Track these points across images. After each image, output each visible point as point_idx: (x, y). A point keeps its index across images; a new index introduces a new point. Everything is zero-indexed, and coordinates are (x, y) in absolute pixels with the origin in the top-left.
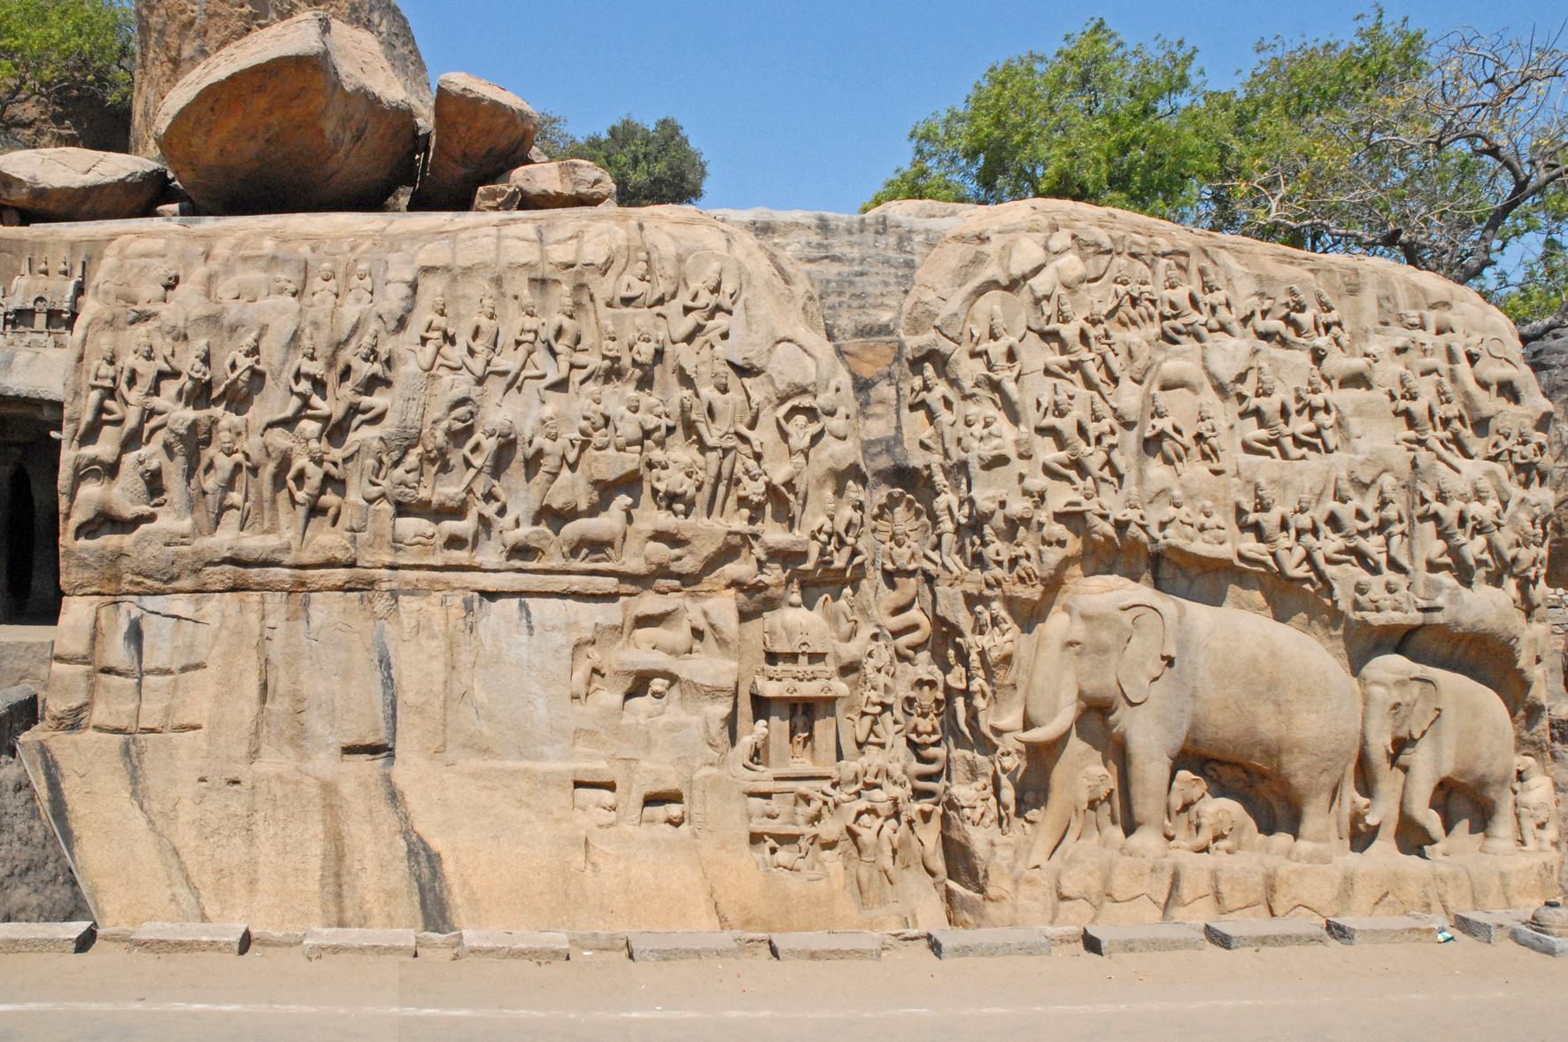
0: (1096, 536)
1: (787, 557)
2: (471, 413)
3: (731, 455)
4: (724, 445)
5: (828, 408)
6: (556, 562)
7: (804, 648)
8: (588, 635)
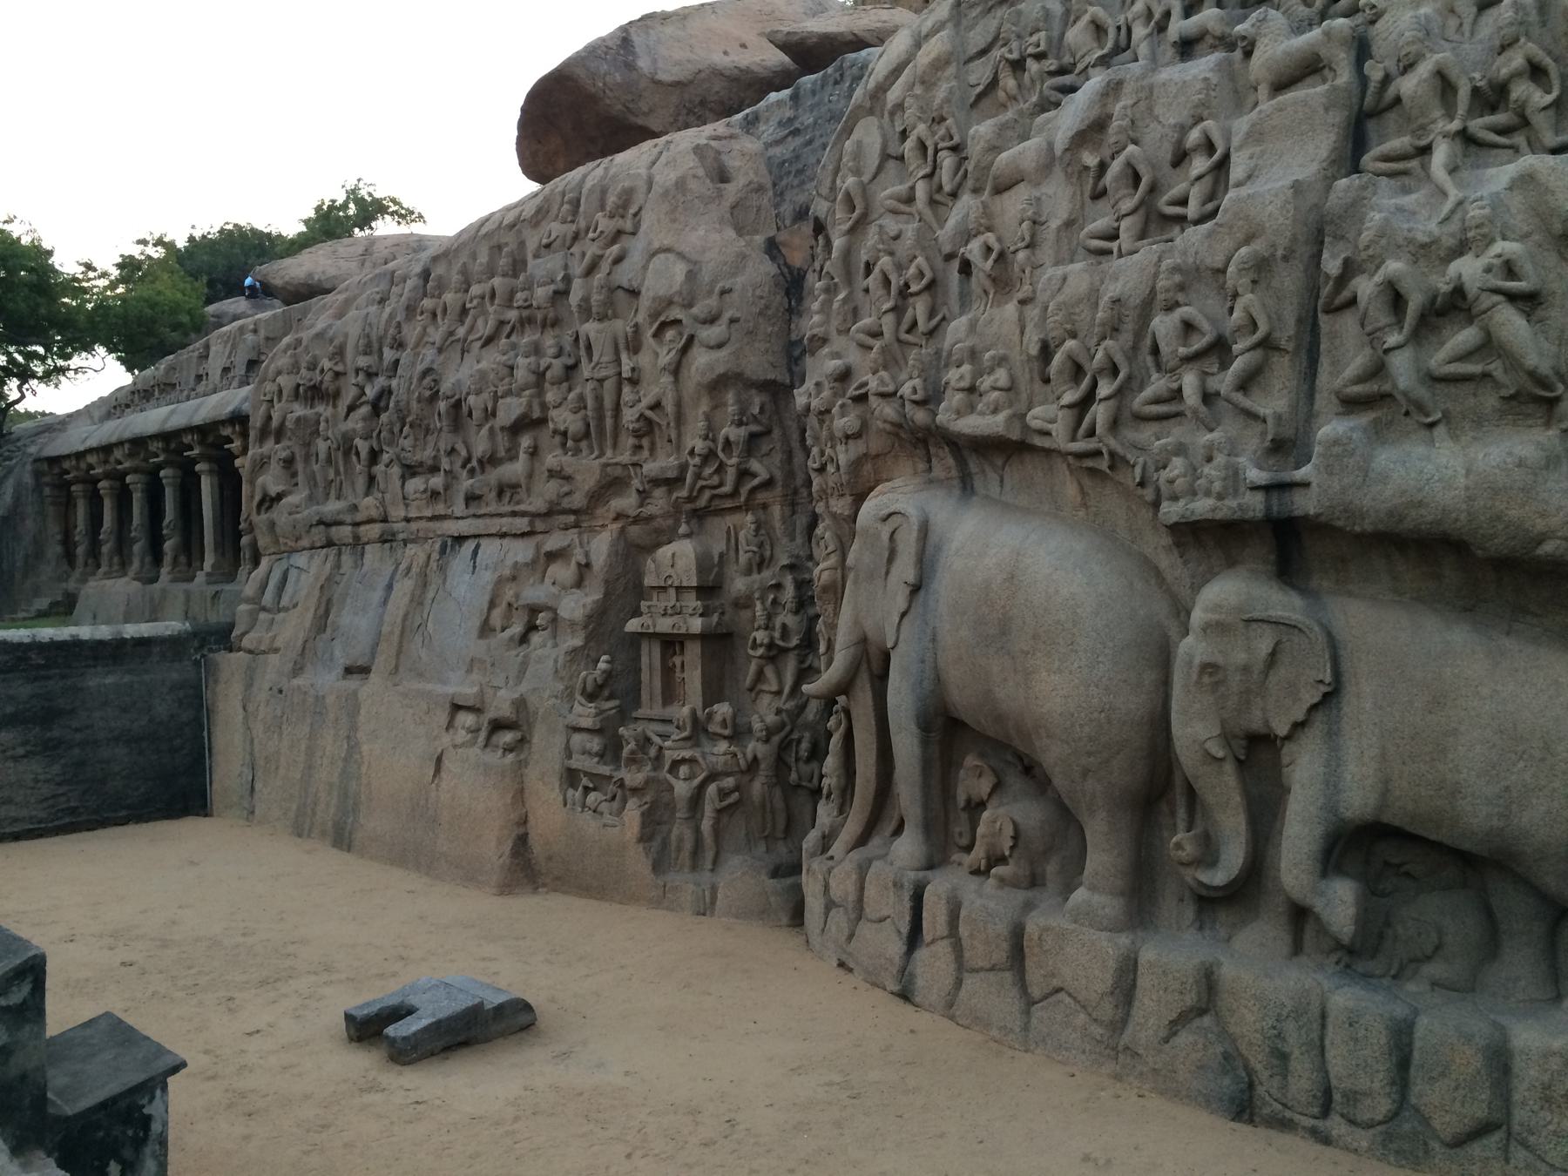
0: (880, 424)
1: (672, 483)
3: (608, 385)
4: (597, 376)
5: (702, 316)
6: (492, 509)
8: (507, 572)
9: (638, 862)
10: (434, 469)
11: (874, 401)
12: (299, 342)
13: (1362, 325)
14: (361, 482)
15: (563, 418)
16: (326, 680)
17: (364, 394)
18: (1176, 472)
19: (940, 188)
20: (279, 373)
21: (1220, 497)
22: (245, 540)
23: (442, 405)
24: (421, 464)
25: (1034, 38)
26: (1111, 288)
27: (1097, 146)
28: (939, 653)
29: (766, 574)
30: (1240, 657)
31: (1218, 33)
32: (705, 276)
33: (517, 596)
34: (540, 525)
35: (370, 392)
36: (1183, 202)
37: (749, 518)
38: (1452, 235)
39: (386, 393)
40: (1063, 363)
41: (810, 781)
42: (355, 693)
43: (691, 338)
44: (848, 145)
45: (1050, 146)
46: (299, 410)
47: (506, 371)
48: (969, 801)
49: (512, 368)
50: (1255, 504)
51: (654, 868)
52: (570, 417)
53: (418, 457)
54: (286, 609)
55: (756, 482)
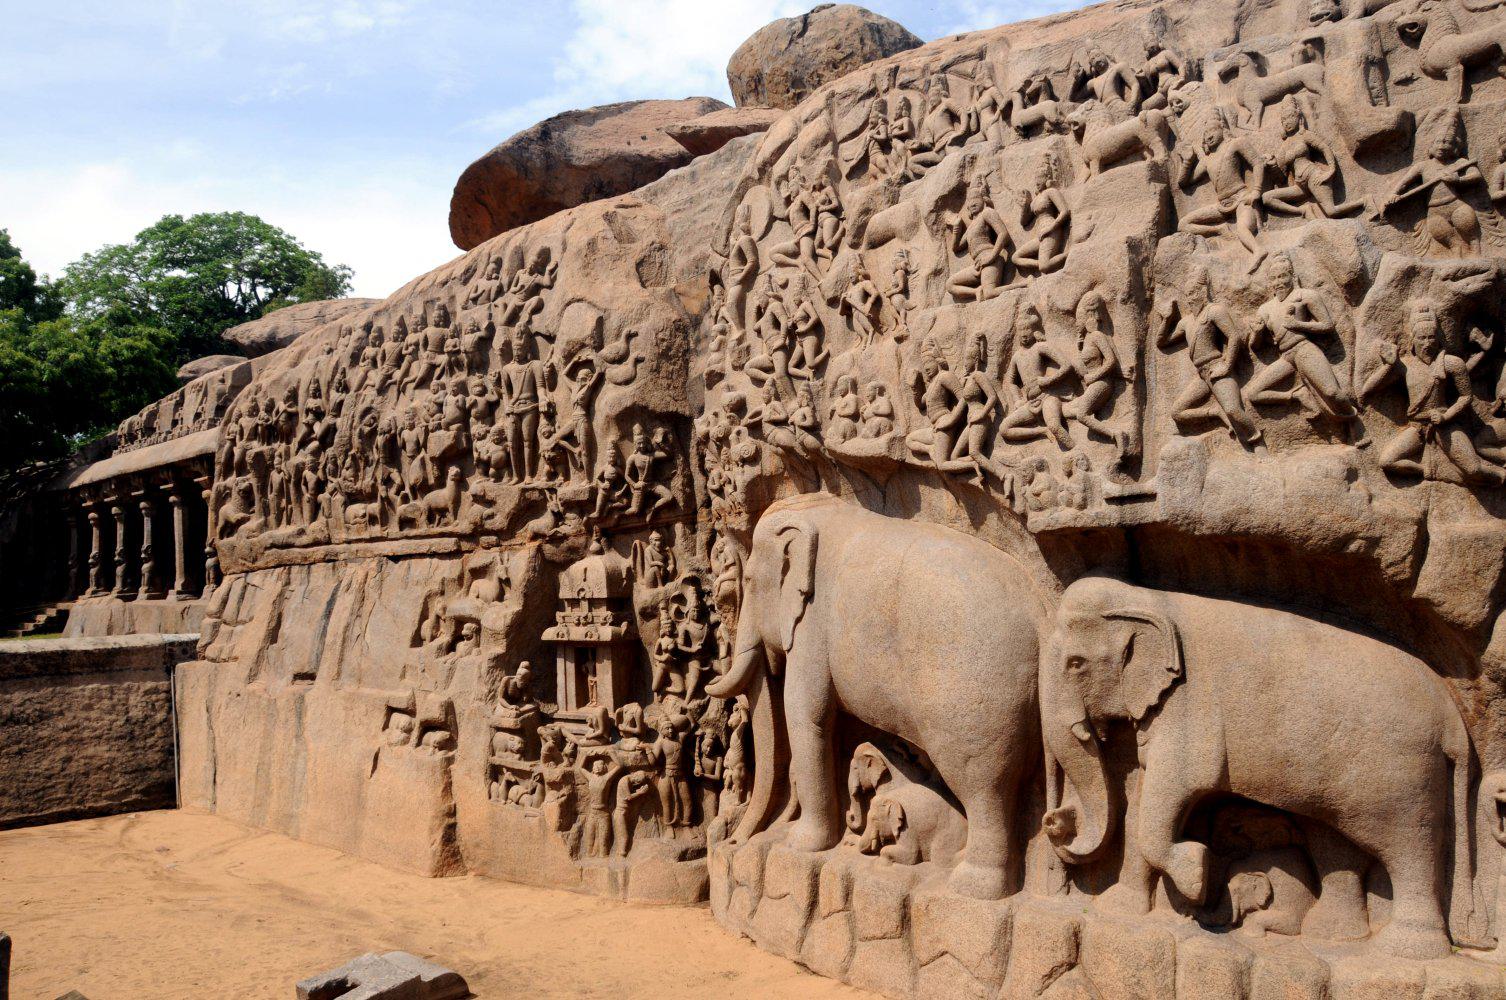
2: (374, 419)
3: (526, 420)
4: (516, 410)
6: (423, 529)
7: (582, 594)
8: (436, 587)
9: (557, 845)
10: (371, 497)
11: (767, 428)
12: (259, 389)
13: (1192, 358)
14: (307, 508)
15: (486, 449)
16: (278, 685)
17: (312, 431)
18: (1041, 486)
19: (822, 244)
20: (240, 416)
21: (1083, 506)
22: (210, 562)
23: (380, 440)
24: (360, 492)
25: (899, 123)
26: (976, 326)
27: (956, 209)
28: (831, 655)
29: (670, 586)
30: (1101, 650)
31: (1053, 120)
32: (611, 325)
33: (444, 609)
34: (465, 546)
35: (318, 428)
36: (1034, 255)
37: (654, 535)
38: (1259, 284)
39: (331, 431)
40: (937, 391)
41: (713, 773)
42: (302, 698)
43: (601, 378)
44: (740, 209)
45: (917, 211)
46: (256, 446)
47: (435, 408)
48: (860, 787)
49: (440, 406)
50: (1112, 515)
51: (571, 855)
52: (494, 447)
53: (358, 485)
54: (244, 623)
55: (659, 503)
